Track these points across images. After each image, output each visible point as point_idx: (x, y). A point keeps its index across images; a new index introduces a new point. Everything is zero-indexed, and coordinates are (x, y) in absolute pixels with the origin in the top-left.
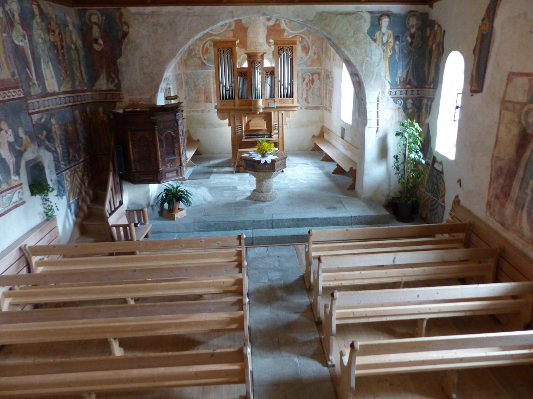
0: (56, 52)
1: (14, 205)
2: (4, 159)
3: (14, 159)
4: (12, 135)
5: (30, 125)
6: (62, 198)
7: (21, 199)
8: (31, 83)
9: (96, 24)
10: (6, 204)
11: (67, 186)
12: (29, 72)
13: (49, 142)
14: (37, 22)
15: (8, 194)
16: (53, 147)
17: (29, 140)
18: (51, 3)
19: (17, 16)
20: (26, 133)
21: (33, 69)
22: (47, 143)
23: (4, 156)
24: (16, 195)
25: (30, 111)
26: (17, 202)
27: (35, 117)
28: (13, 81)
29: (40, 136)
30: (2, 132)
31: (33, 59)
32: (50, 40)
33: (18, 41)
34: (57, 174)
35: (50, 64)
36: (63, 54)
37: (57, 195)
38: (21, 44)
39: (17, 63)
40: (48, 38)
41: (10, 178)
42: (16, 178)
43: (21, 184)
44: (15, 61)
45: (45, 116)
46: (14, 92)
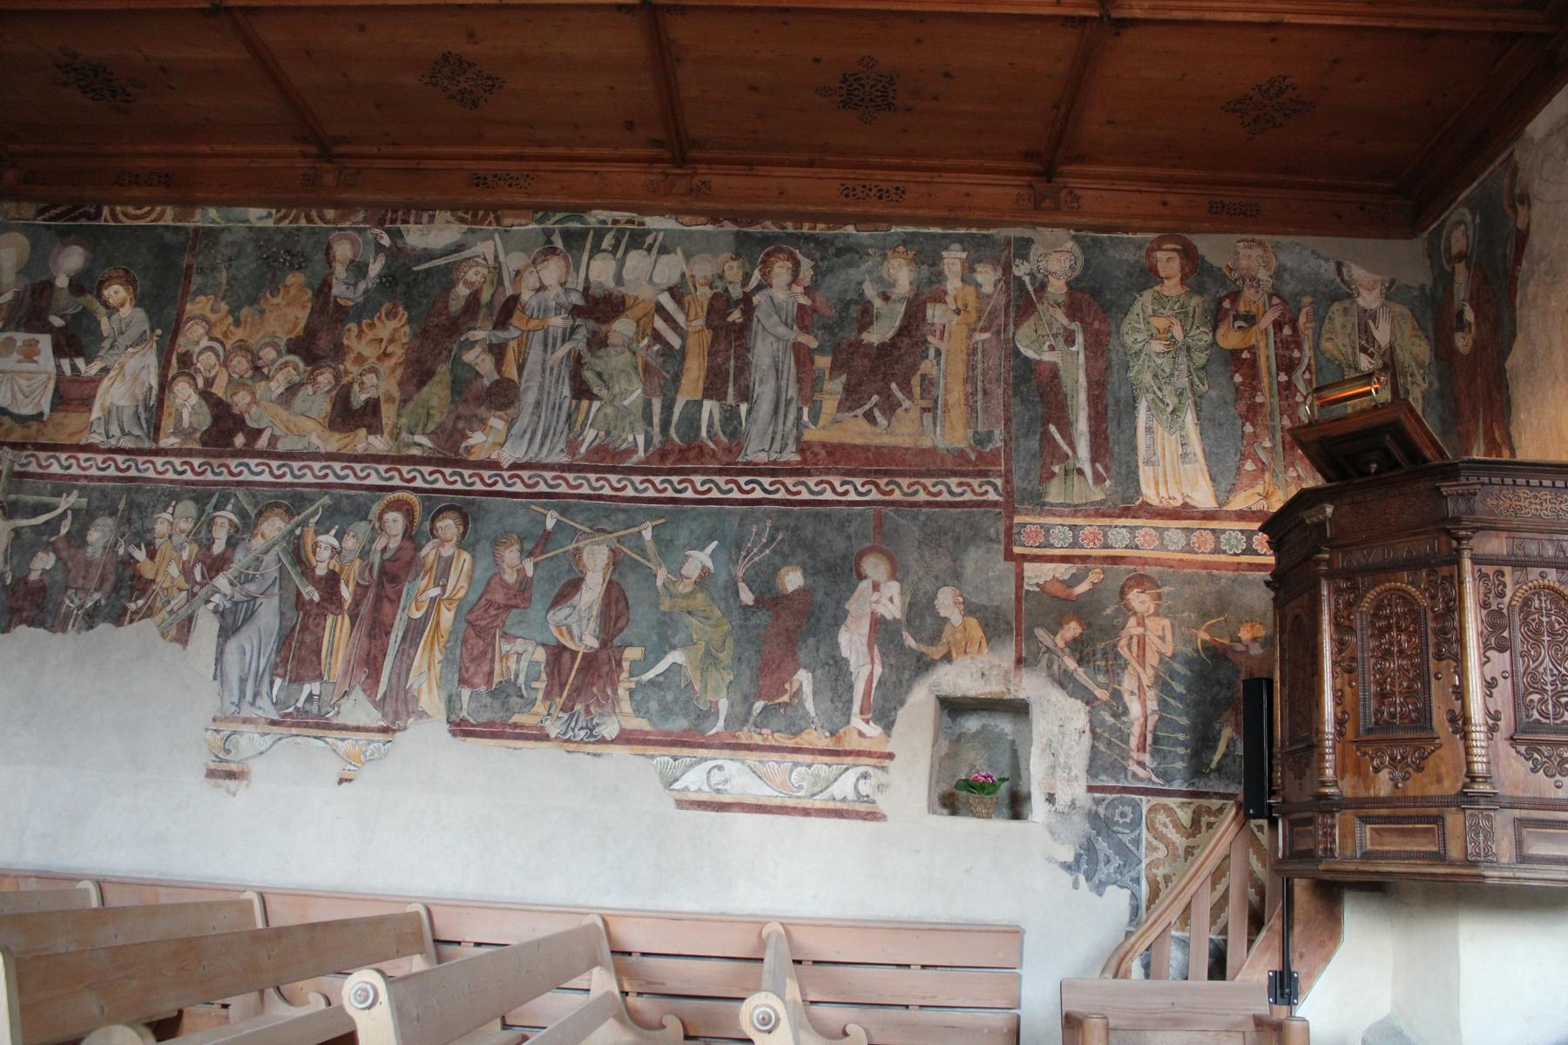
0: (1238, 378)
1: (831, 805)
2: (846, 661)
3: (878, 670)
4: (897, 600)
5: (1009, 589)
6: (1099, 888)
7: (867, 799)
8: (1056, 469)
9: (1461, 256)
10: (800, 788)
11: (1151, 856)
12: (1058, 437)
13: (1080, 662)
14: (1160, 299)
15: (822, 767)
16: (1105, 687)
17: (977, 633)
18: (1257, 237)
19: (1057, 287)
20: (969, 610)
21: (1082, 425)
22: (1071, 664)
23: (845, 653)
24: (850, 777)
25: (1017, 550)
26: (844, 800)
27: (1038, 574)
28: (973, 457)
29: (1040, 633)
30: (864, 585)
31: (1095, 400)
32: (1214, 343)
33: (1039, 351)
34: (1090, 789)
35: (1189, 417)
36: (1288, 389)
37: (1068, 867)
38: (1047, 357)
39: (1017, 408)
40: (1208, 338)
41: (848, 722)
42: (873, 730)
43: (891, 756)
44: (1006, 407)
45: (1095, 576)
46: (960, 484)
